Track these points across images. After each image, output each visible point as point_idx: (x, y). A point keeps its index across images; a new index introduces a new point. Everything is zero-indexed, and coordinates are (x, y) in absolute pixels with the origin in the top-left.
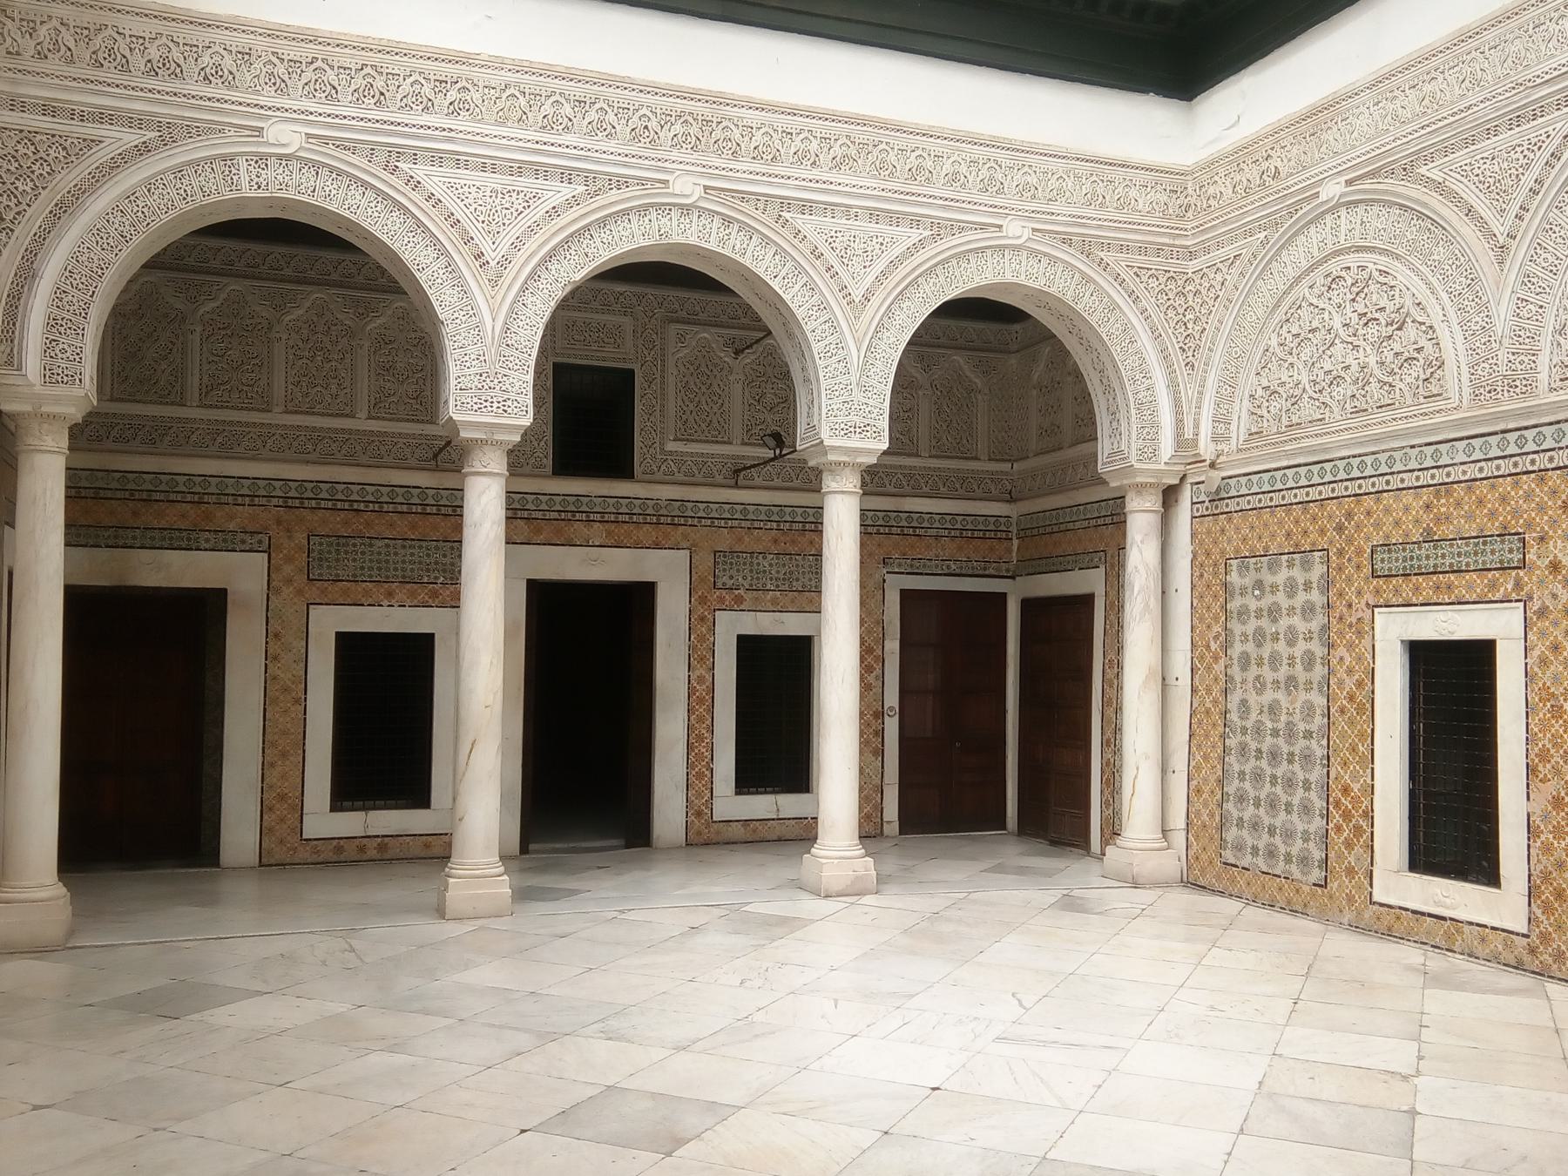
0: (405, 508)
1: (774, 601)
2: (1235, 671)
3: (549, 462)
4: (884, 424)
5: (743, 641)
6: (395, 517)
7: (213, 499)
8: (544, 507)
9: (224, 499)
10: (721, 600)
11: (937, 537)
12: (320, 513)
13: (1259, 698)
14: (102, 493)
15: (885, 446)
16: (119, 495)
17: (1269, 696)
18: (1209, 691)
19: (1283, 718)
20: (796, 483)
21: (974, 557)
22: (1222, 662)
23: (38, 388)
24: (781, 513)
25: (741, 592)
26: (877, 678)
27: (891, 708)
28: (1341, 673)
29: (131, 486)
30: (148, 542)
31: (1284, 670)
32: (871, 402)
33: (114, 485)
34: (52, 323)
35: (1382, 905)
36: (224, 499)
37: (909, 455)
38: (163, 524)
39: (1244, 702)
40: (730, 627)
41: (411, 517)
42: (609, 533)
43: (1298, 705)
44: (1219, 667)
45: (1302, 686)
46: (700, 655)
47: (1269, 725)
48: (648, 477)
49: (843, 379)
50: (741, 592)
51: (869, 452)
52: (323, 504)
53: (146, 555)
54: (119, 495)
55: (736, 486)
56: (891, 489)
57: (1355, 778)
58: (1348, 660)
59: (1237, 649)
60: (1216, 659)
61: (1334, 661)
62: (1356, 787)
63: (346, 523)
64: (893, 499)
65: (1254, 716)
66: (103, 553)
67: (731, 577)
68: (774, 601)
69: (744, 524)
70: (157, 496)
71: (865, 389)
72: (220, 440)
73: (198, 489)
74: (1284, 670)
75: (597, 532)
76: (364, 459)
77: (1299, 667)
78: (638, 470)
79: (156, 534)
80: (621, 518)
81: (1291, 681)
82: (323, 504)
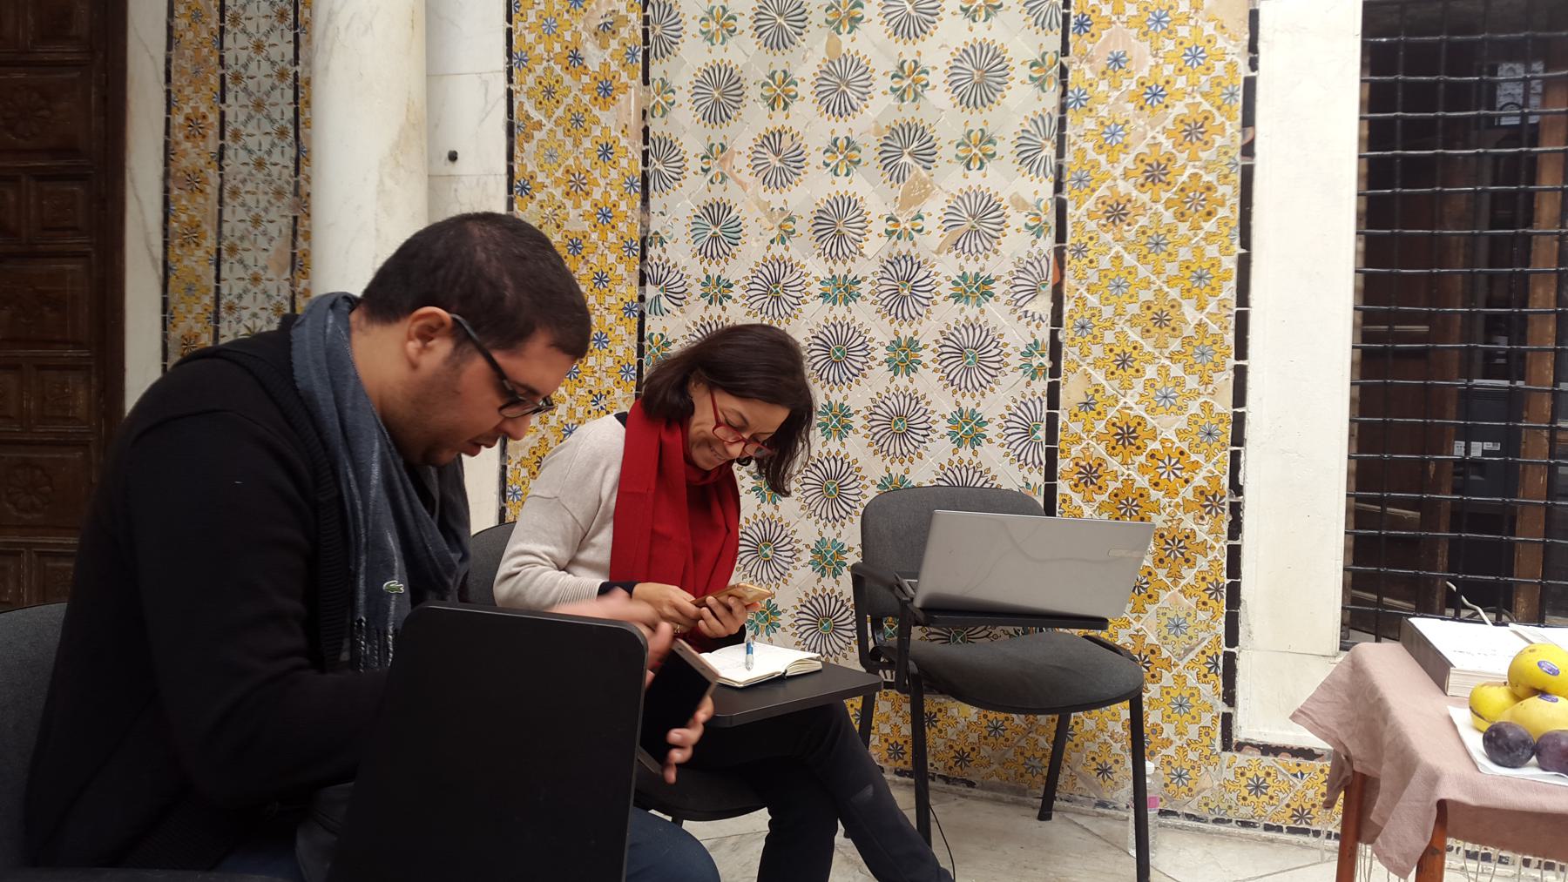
2: (684, 126)
13: (776, 199)
17: (814, 189)
18: (577, 185)
19: (875, 246)
22: (630, 100)
28: (1108, 100)
31: (878, 110)
35: (1267, 750)
39: (715, 213)
43: (934, 208)
44: (617, 120)
45: (946, 152)
47: (817, 268)
57: (1167, 400)
58: (1144, 65)
59: (689, 60)
60: (606, 91)
61: (1081, 74)
62: (1168, 428)
65: (753, 250)
74: (878, 110)
77: (939, 97)
81: (906, 147)
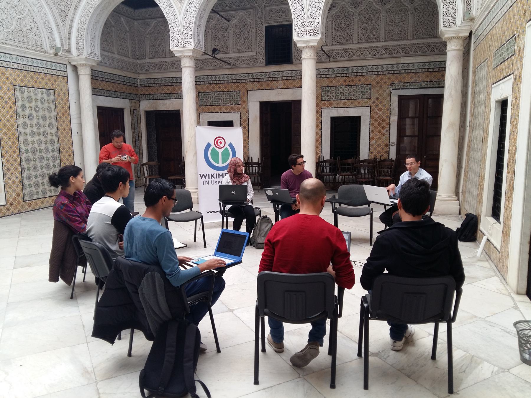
0: (223, 82)
1: (344, 104)
3: (264, 61)
4: (319, 29)
5: (333, 119)
6: (221, 85)
7: (175, 84)
8: (263, 77)
9: (177, 84)
10: (324, 104)
11: (416, 73)
12: (201, 86)
14: (150, 85)
15: (320, 37)
16: (154, 85)
20: (354, 58)
21: (434, 79)
23: (76, 58)
24: (333, 71)
25: (332, 101)
26: (387, 131)
27: (393, 143)
29: (156, 82)
30: (161, 98)
32: (313, 20)
33: (152, 82)
34: (78, 39)
36: (177, 84)
37: (403, 40)
38: (164, 92)
40: (328, 114)
41: (225, 85)
42: (284, 84)
46: (319, 125)
48: (297, 62)
49: (301, 13)
50: (332, 101)
51: (313, 41)
52: (202, 83)
53: (161, 102)
54: (154, 85)
55: (330, 62)
56: (394, 55)
63: (208, 88)
64: (395, 59)
66: (152, 102)
67: (328, 96)
68: (344, 104)
69: (333, 76)
70: (162, 85)
71: (310, 16)
72: (175, 66)
73: (171, 82)
75: (280, 84)
76: (211, 68)
78: (294, 60)
79: (162, 95)
80: (288, 78)
82: (202, 83)
